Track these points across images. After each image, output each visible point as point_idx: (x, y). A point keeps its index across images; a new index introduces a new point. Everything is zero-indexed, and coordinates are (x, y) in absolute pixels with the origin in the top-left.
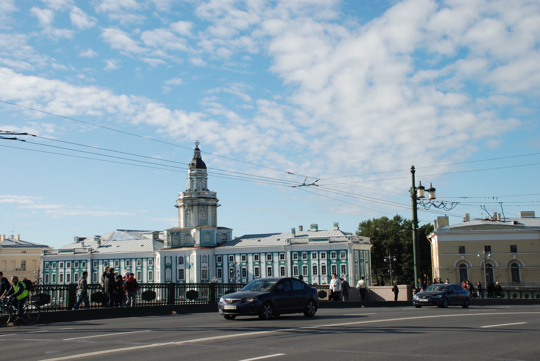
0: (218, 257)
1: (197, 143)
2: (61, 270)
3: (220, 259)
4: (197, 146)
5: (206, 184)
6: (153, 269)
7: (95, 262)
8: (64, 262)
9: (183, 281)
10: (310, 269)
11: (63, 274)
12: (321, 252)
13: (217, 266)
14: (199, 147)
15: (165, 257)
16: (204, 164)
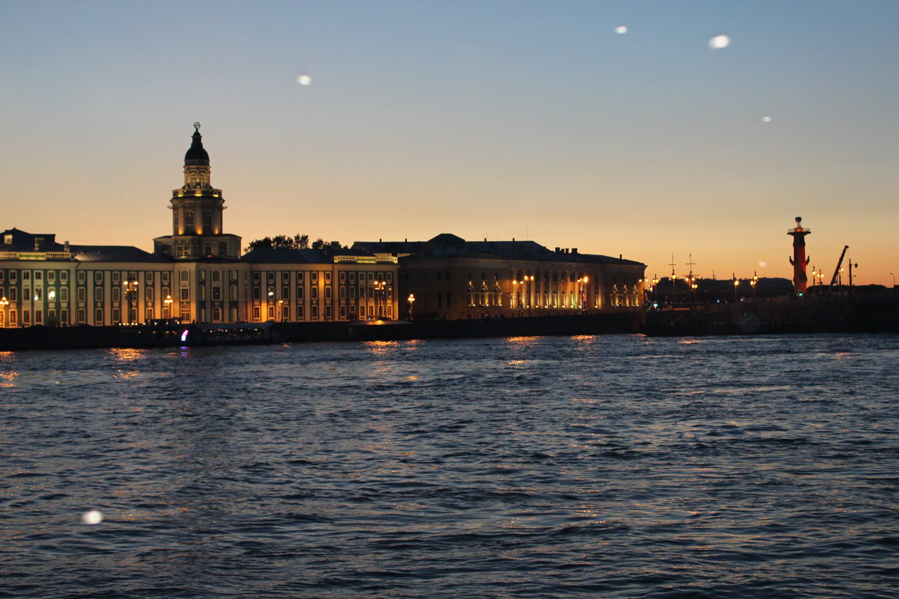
0: (255, 274)
1: (197, 126)
2: (26, 283)
3: (256, 276)
4: (197, 130)
5: (209, 179)
6: (169, 286)
7: (80, 274)
8: (30, 272)
9: (220, 302)
10: (357, 291)
11: (30, 288)
12: (368, 273)
13: (253, 285)
14: (200, 131)
15: (199, 271)
16: (207, 153)
